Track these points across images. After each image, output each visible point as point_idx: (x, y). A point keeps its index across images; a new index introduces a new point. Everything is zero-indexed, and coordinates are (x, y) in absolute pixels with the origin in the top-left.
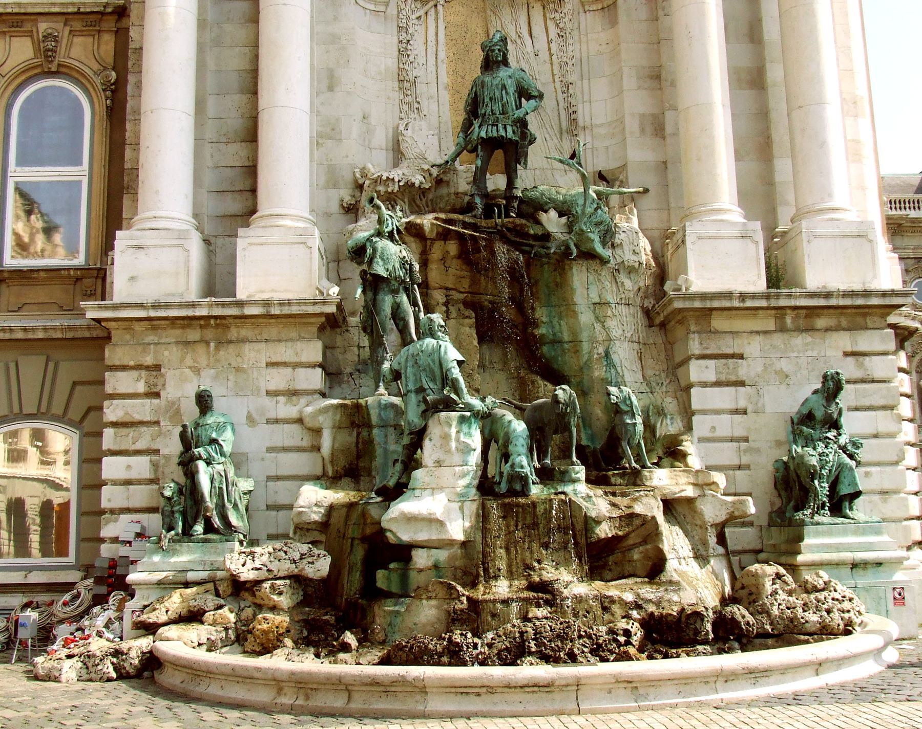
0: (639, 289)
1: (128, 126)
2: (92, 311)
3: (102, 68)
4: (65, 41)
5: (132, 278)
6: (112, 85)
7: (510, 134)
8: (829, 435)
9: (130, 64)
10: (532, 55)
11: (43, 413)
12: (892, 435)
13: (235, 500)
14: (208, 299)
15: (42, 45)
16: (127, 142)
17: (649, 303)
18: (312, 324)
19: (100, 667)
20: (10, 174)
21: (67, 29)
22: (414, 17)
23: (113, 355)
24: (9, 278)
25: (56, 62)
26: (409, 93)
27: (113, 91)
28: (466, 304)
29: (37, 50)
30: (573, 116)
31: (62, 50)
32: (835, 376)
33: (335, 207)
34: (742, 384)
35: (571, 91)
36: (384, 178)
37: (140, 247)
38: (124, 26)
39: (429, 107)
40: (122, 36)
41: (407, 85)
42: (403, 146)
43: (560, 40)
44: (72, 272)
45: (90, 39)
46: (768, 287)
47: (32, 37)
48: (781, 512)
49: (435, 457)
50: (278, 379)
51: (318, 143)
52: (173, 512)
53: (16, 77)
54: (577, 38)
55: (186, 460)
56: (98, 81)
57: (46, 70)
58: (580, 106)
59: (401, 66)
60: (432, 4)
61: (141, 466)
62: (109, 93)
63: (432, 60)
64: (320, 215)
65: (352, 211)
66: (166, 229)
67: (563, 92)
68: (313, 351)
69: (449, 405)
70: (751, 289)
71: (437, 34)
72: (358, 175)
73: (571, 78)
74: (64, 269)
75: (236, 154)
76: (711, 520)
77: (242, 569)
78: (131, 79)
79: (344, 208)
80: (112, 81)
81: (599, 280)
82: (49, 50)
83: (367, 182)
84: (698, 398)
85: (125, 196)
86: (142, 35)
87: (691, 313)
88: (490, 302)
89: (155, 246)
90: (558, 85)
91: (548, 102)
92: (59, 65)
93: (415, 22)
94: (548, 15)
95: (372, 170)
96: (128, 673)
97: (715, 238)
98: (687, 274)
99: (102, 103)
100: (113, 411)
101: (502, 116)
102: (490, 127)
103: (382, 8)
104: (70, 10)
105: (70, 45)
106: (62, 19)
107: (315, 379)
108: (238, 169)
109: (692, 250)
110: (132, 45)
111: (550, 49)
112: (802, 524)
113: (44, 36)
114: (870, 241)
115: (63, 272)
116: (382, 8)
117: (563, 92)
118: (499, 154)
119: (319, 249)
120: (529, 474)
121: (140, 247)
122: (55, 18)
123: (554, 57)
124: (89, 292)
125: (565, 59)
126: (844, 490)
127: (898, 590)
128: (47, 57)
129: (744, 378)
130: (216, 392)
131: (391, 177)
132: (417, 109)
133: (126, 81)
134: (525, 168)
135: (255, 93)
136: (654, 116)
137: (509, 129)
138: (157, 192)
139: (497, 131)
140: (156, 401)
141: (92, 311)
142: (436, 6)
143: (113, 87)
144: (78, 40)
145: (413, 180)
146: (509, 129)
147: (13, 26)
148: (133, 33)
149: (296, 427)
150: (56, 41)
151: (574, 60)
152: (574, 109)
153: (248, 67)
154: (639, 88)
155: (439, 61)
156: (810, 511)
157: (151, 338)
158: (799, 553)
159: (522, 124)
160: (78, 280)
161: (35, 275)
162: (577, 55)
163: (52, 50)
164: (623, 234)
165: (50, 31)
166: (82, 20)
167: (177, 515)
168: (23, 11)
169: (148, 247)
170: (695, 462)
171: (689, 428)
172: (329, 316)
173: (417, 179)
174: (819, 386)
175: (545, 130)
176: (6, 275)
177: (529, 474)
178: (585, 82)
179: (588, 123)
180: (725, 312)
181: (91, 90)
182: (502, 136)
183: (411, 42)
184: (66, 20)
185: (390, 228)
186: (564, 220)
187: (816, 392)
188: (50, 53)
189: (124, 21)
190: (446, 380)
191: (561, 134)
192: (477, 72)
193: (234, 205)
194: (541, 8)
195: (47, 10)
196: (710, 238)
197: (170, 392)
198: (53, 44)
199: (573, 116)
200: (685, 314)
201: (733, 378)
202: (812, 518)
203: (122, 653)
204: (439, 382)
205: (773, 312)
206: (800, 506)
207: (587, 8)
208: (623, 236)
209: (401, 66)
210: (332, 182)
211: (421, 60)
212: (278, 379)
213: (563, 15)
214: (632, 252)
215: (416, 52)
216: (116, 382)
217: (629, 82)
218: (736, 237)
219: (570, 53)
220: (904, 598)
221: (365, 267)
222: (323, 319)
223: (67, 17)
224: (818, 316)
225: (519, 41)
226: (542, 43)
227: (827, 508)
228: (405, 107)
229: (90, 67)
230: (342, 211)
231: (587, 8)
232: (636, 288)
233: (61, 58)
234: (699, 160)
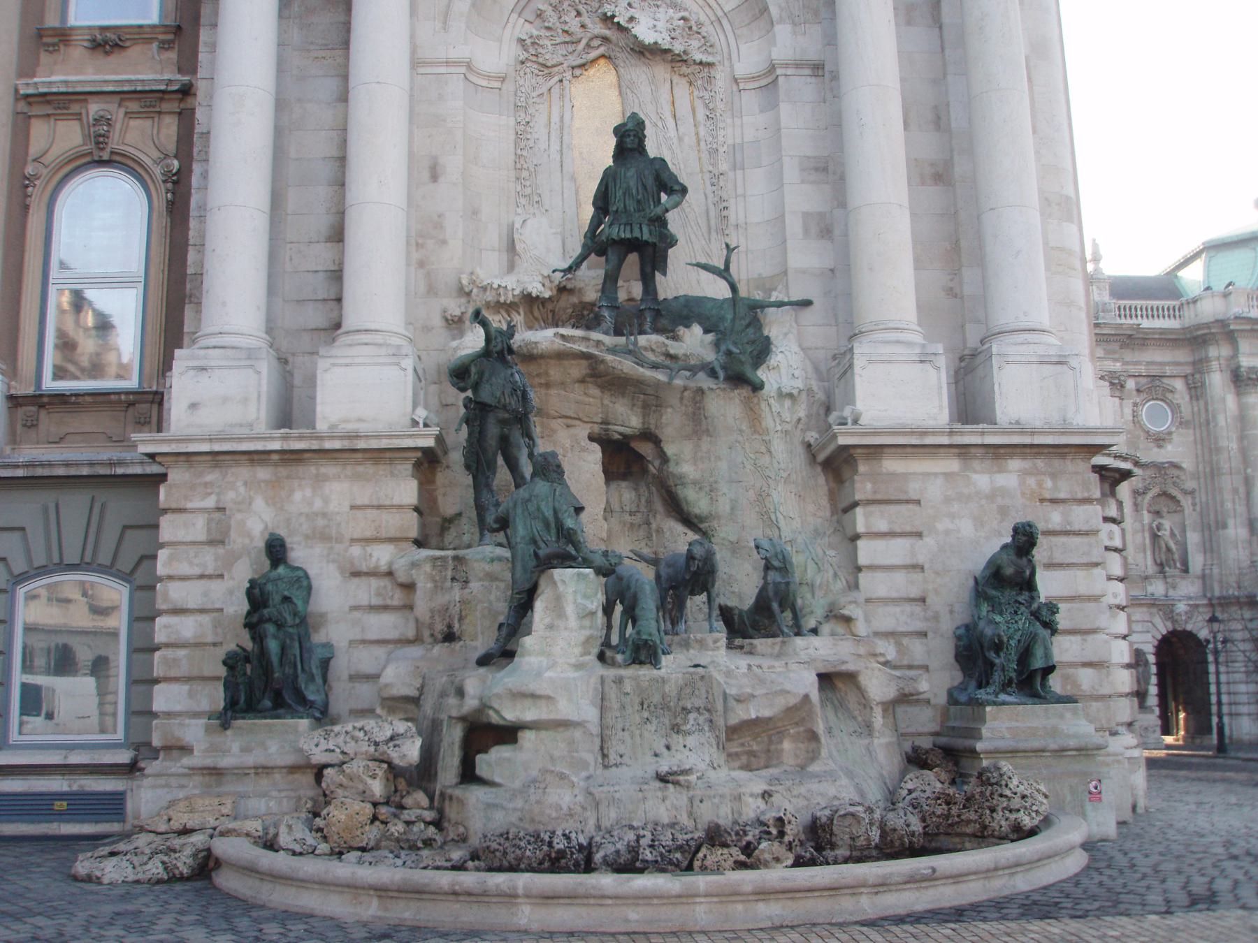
0: (799, 420)
1: (193, 224)
2: (146, 443)
3: (162, 156)
4: (118, 126)
5: (194, 406)
6: (174, 175)
7: (646, 237)
8: (1021, 599)
9: (196, 150)
10: (675, 141)
11: (87, 563)
12: (1096, 599)
13: (310, 668)
14: (282, 431)
15: (92, 130)
16: (191, 242)
17: (812, 436)
18: (406, 459)
19: (148, 867)
20: (51, 281)
21: (122, 112)
22: (534, 94)
24: (49, 404)
25: (108, 150)
26: (528, 183)
27: (174, 183)
28: (592, 438)
29: (87, 137)
30: (725, 213)
31: (115, 135)
32: (1027, 528)
33: (437, 321)
34: (919, 535)
35: (722, 184)
36: (495, 286)
37: (203, 369)
38: (189, 106)
40: (187, 119)
41: (525, 174)
42: (519, 246)
43: (708, 123)
44: (123, 397)
45: (148, 123)
46: (952, 420)
47: (80, 120)
48: (962, 688)
49: (547, 621)
51: (417, 244)
52: (238, 684)
53: (61, 167)
54: (729, 121)
55: (255, 619)
56: (157, 171)
57: (96, 158)
58: (732, 201)
59: (519, 152)
60: (556, 79)
62: (170, 185)
63: (555, 147)
66: (233, 348)
67: (713, 185)
68: (406, 490)
69: (565, 560)
70: (931, 423)
71: (562, 118)
72: (465, 282)
73: (724, 166)
74: (114, 393)
76: (878, 699)
77: (316, 751)
78: (197, 168)
79: (447, 320)
80: (174, 171)
81: (751, 409)
82: (100, 136)
83: (475, 290)
84: (867, 551)
85: (187, 306)
86: (210, 118)
87: (859, 451)
88: (620, 434)
89: (220, 367)
90: (707, 176)
91: (694, 199)
92: (112, 153)
93: (537, 100)
94: (696, 93)
95: (482, 276)
96: (181, 874)
97: (889, 362)
98: (854, 404)
99: (162, 196)
101: (637, 215)
102: (622, 227)
103: (497, 85)
104: (125, 89)
105: (125, 130)
106: (117, 98)
108: (321, 274)
109: (861, 376)
110: (198, 129)
111: (697, 134)
112: (982, 704)
113: (95, 120)
114: (1073, 369)
115: (113, 397)
116: (497, 85)
117: (713, 185)
118: (633, 258)
119: (415, 370)
120: (658, 642)
121: (203, 369)
122: (108, 98)
123: (702, 143)
124: (142, 420)
125: (715, 146)
126: (1038, 663)
127: (1094, 783)
128: (98, 143)
129: (921, 529)
131: (503, 285)
132: (537, 202)
133: (191, 171)
134: (664, 274)
135: (343, 185)
136: (821, 215)
137: (645, 229)
138: (224, 304)
139: (632, 232)
140: (220, 550)
141: (146, 443)
142: (561, 81)
143: (175, 178)
144: (134, 123)
145: (530, 290)
146: (645, 229)
147: (59, 108)
148: (199, 114)
149: (385, 582)
150: (109, 125)
151: (725, 148)
152: (725, 204)
153: (335, 153)
154: (803, 182)
155: (564, 146)
156: (993, 688)
157: (211, 477)
158: (980, 738)
159: (661, 222)
160: (131, 404)
161: (80, 399)
162: (730, 142)
163: (103, 136)
164: (780, 355)
165: (102, 113)
166: (139, 99)
167: (241, 687)
168: (70, 90)
169: (212, 368)
170: (861, 628)
171: (855, 586)
172: (427, 452)
173: (536, 288)
174: (1009, 540)
175: (690, 230)
176: (45, 400)
177: (658, 642)
178: (739, 173)
179: (741, 221)
180: (899, 450)
181: (149, 181)
182: (637, 238)
183: (531, 124)
184: (122, 100)
185: (499, 348)
186: (710, 337)
187: (1005, 547)
188: (101, 139)
189: (189, 100)
191: (709, 233)
192: (610, 162)
193: (315, 317)
194: (688, 85)
195: (98, 89)
196: (883, 362)
197: (236, 541)
198: (105, 128)
199: (725, 213)
200: (852, 451)
201: (908, 529)
202: (997, 697)
203: (175, 851)
204: (553, 531)
205: (956, 451)
206: (984, 682)
207: (742, 86)
208: (780, 357)
209: (519, 152)
210: (431, 290)
211: (543, 145)
212: (363, 525)
213: (713, 94)
214: (790, 376)
215: (536, 136)
217: (791, 173)
218: (914, 362)
219: (720, 138)
220: (1100, 793)
221: (469, 393)
222: (419, 454)
223: (123, 96)
224: (1011, 456)
225: (660, 124)
226: (687, 127)
227: (1014, 685)
228: (523, 201)
230: (444, 324)
231: (742, 86)
232: (795, 420)
233: (115, 143)
234: (871, 269)
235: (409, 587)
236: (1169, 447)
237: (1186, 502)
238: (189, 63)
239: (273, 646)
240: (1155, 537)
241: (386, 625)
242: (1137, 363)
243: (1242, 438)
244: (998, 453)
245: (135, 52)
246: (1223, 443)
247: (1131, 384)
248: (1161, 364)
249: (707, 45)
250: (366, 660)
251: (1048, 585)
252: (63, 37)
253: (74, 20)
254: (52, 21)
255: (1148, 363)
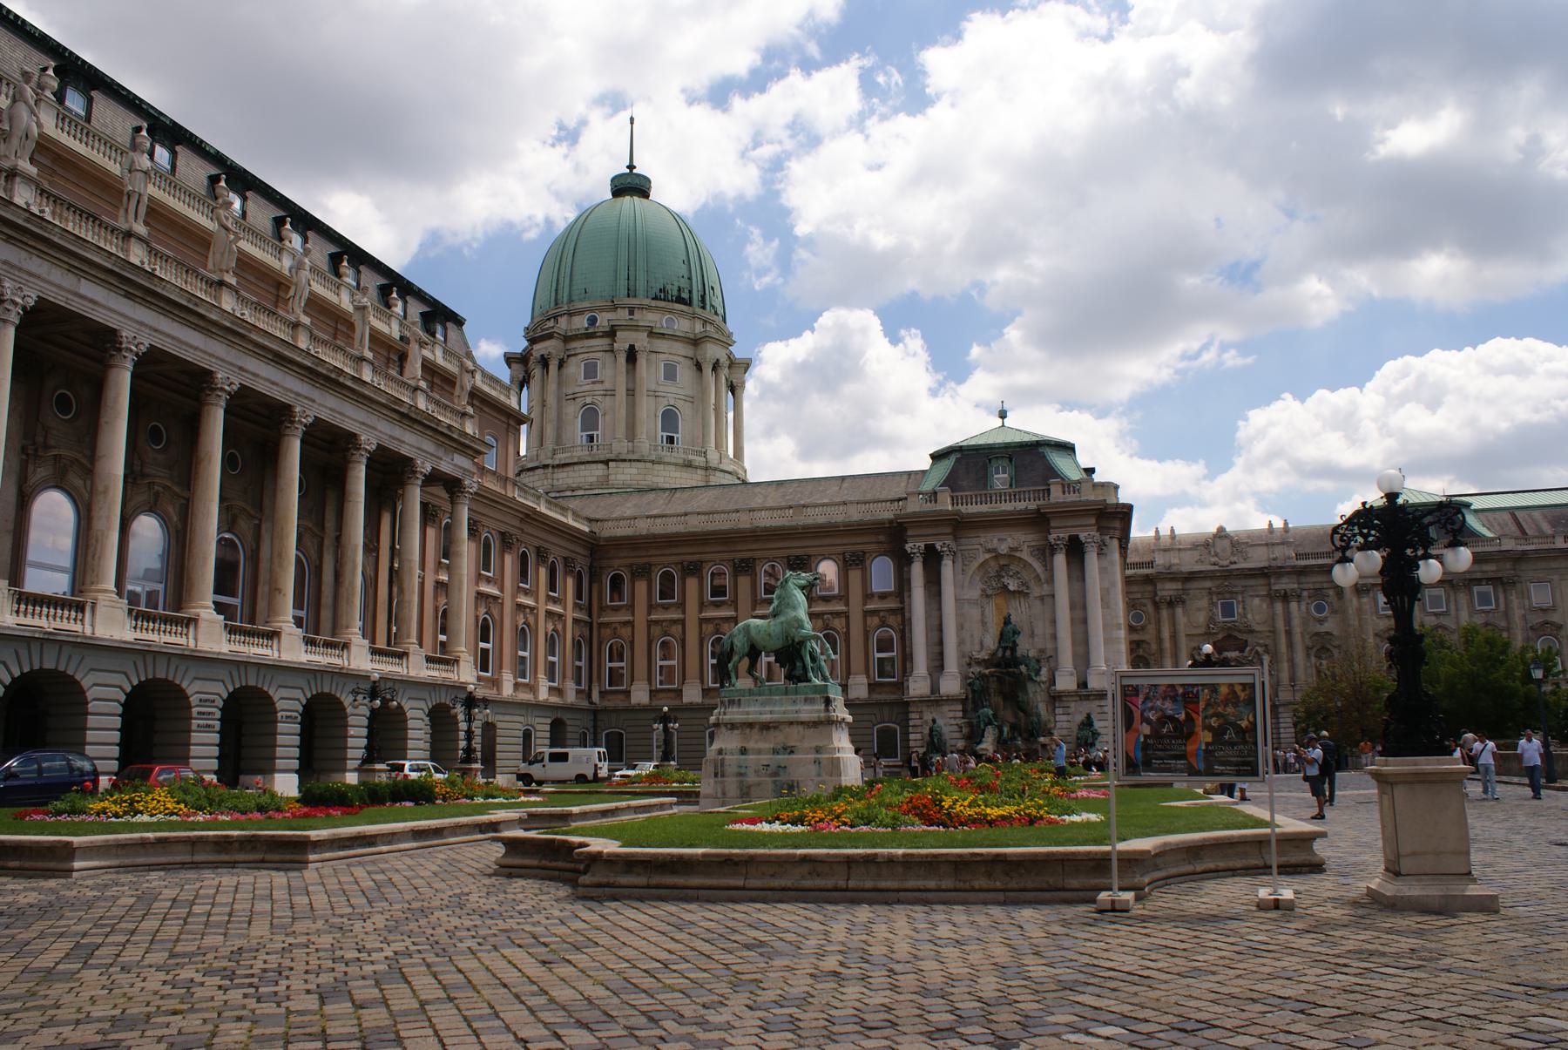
23: (910, 709)
39: (991, 630)
40: (903, 615)
50: (952, 714)
61: (919, 736)
64: (960, 666)
65: (969, 665)
68: (960, 707)
69: (990, 723)
75: (936, 649)
99: (899, 635)
100: (911, 723)
107: (960, 714)
130: (937, 718)
159: (1014, 642)
190: (990, 719)
193: (937, 663)
197: (925, 718)
210: (963, 656)
212: (952, 714)
216: (912, 716)
229: (895, 624)
235: (961, 727)
236: (1326, 624)
237: (1335, 652)
238: (902, 602)
239: (936, 741)
240: (1319, 672)
241: (957, 735)
242: (1308, 583)
243: (1360, 620)
244: (1087, 697)
245: (889, 599)
246: (1351, 622)
247: (1305, 594)
248: (1322, 582)
249: (1028, 588)
250: (953, 742)
251: (1097, 725)
252: (872, 595)
253: (874, 590)
254: (869, 592)
255: (1314, 583)
